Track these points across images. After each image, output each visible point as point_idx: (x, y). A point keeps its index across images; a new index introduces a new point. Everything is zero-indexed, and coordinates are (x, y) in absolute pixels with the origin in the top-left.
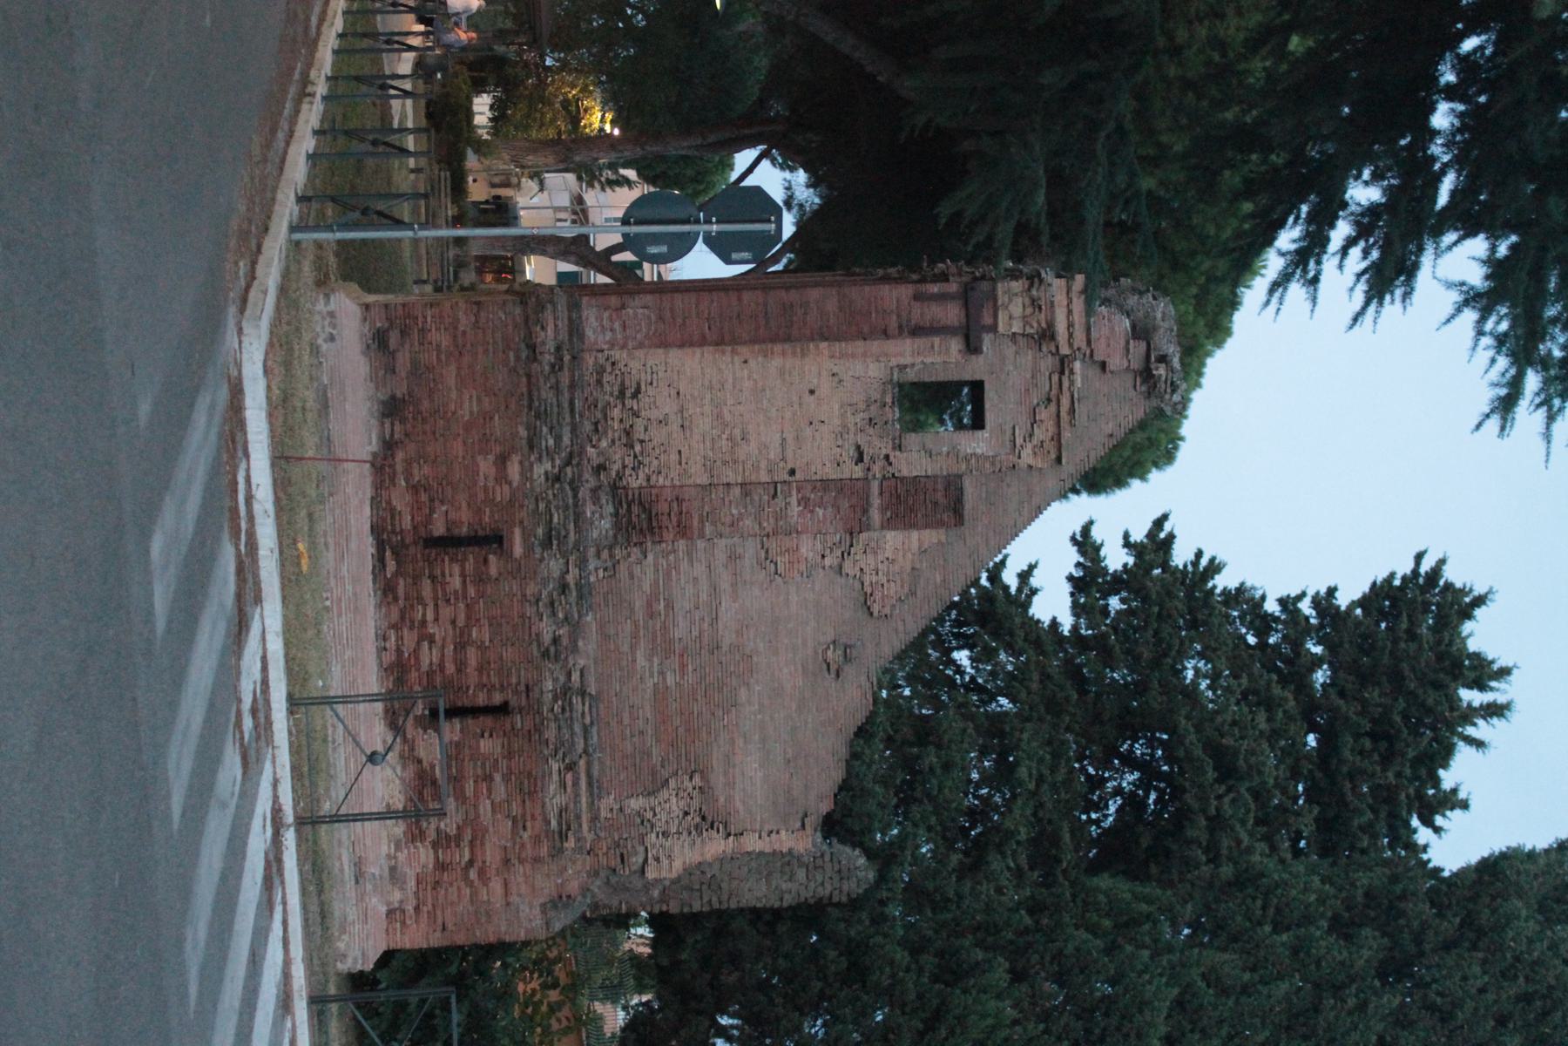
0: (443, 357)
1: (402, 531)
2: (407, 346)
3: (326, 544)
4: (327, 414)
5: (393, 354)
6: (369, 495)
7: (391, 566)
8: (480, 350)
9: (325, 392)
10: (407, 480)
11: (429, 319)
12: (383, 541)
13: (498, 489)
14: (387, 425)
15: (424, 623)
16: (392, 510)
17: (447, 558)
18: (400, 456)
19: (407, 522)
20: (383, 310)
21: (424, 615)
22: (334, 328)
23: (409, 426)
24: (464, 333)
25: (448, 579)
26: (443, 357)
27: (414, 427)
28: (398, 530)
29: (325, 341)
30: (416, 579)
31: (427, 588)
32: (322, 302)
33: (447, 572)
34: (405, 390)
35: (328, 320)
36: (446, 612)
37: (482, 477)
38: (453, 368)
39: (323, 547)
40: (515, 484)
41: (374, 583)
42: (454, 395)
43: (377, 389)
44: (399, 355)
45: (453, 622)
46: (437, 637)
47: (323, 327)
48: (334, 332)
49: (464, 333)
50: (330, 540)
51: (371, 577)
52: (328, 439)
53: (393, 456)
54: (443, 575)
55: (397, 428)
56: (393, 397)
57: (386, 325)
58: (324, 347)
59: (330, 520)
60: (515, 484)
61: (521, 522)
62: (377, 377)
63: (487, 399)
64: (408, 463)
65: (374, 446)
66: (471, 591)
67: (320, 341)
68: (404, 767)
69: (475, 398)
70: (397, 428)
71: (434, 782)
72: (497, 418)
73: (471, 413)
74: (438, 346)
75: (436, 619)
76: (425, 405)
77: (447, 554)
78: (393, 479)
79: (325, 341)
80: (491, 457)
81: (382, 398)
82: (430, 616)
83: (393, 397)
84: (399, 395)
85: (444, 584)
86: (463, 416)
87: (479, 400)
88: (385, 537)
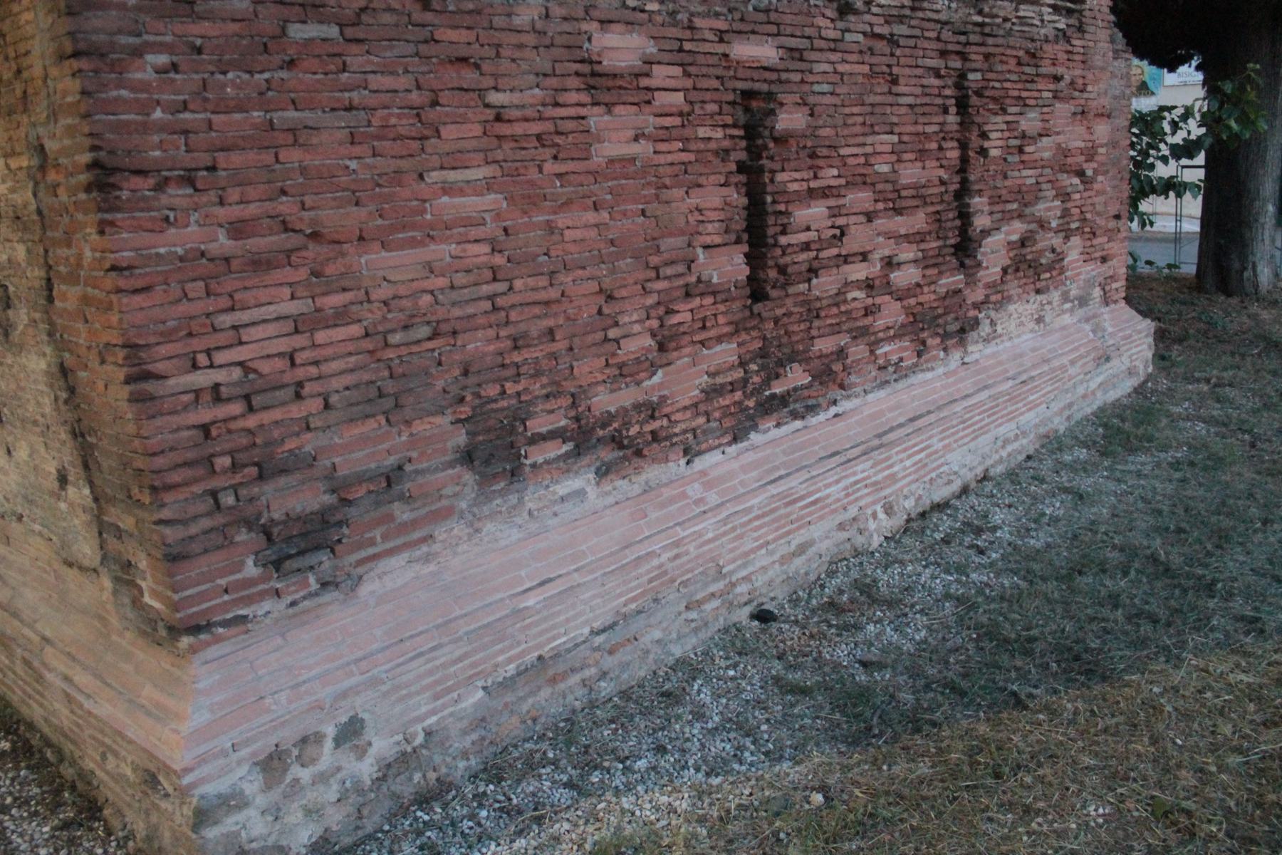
1: (742, 364)
2: (309, 443)
3: (802, 549)
4: (556, 656)
5: (340, 488)
6: (677, 466)
7: (796, 376)
8: (293, 156)
9: (507, 684)
10: (653, 368)
11: (202, 379)
12: (759, 404)
13: (662, 99)
14: (537, 455)
15: (869, 285)
16: (711, 393)
17: (783, 240)
18: (605, 401)
19: (726, 353)
20: (202, 565)
21: (857, 285)
22: (338, 742)
23: (537, 388)
24: (238, 229)
25: (812, 235)
27: (537, 374)
28: (739, 374)
30: (812, 312)
31: (825, 284)
32: (230, 823)
33: (803, 237)
34: (444, 421)
35: (296, 771)
36: (859, 237)
38: (372, 261)
39: (811, 552)
40: (651, 49)
41: (812, 409)
42: (443, 251)
43: (447, 513)
44: (347, 465)
45: (870, 217)
46: (887, 252)
47: (322, 778)
48: (330, 731)
49: (238, 229)
50: (797, 540)
51: (813, 420)
52: (612, 627)
53: (606, 420)
54: (806, 247)
55: (539, 424)
56: (468, 457)
57: (242, 536)
58: (382, 745)
59: (762, 559)
60: (651, 49)
61: (721, 37)
62: (414, 524)
63: (448, 132)
64: (624, 373)
65: (581, 480)
66: (830, 175)
67: (366, 769)
68: (1009, 299)
69: (452, 176)
70: (539, 424)
71: (1023, 243)
72: (495, 98)
73: (489, 186)
74: (299, 325)
75: (864, 256)
76: (478, 344)
77: (774, 236)
78: (651, 410)
79: (361, 752)
80: (597, 119)
81: (470, 492)
82: (858, 272)
83: (468, 457)
85: (822, 244)
86: (498, 216)
87: (453, 162)
88: (751, 403)
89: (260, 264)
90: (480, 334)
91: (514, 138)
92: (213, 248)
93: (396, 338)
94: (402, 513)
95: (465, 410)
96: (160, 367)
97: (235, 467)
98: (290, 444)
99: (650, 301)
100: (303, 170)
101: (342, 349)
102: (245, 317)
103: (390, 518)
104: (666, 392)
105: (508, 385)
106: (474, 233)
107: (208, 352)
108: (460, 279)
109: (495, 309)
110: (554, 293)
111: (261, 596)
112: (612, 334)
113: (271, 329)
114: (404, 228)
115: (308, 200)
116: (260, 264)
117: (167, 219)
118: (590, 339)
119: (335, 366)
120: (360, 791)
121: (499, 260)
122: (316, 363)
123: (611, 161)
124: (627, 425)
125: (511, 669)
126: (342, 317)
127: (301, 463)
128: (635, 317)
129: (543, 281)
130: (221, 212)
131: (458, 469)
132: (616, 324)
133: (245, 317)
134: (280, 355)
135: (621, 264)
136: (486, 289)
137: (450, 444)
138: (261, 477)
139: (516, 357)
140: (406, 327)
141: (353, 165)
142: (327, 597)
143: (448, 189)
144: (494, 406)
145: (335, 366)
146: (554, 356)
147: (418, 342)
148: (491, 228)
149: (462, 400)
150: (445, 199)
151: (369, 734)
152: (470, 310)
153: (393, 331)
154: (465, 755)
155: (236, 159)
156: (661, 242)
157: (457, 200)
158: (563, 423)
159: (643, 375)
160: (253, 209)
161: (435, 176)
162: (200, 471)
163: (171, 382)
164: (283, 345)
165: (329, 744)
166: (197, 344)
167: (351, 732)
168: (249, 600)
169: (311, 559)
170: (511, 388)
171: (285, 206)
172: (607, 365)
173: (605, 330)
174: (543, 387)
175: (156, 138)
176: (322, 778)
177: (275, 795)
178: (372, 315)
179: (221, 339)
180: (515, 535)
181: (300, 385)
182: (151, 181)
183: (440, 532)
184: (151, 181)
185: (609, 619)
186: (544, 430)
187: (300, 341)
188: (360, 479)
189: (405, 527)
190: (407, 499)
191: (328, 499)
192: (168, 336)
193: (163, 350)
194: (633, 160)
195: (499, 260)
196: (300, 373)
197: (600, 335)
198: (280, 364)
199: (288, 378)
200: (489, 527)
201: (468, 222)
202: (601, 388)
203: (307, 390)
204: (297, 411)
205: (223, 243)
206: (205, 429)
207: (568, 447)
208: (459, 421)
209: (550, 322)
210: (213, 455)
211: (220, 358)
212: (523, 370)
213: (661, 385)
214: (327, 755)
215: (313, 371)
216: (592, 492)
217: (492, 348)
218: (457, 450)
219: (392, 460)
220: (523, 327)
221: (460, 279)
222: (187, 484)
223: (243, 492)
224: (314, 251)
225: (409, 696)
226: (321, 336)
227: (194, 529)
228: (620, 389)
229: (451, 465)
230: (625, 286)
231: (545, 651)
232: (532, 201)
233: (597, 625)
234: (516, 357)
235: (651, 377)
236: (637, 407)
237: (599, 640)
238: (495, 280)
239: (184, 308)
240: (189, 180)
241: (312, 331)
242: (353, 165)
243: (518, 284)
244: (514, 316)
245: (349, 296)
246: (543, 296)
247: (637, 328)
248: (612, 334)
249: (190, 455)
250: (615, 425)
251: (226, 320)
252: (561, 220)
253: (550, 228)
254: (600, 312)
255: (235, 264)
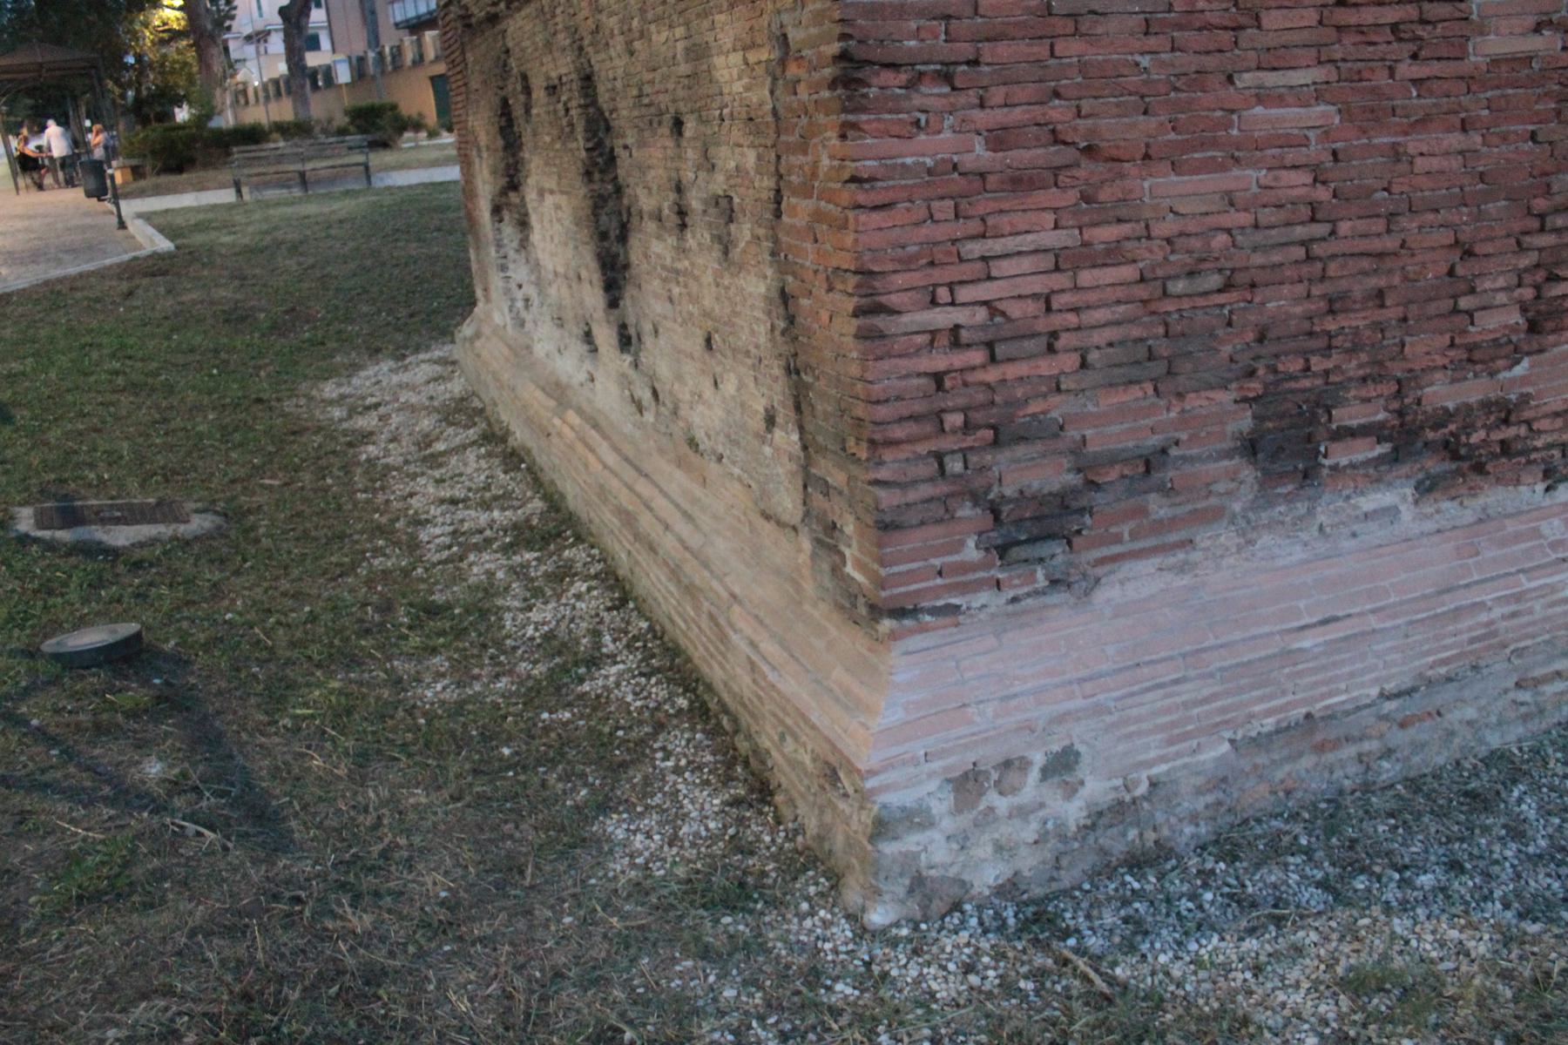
0: (1105, 234)
2: (1058, 408)
4: (1330, 716)
5: (1088, 468)
6: (1531, 492)
8: (1071, 49)
9: (1260, 742)
11: (942, 318)
14: (1342, 455)
18: (1441, 393)
20: (912, 541)
22: (1046, 773)
23: (1352, 367)
26: (1105, 234)
27: (1352, 351)
29: (1071, 790)
32: (911, 842)
34: (1226, 397)
35: (993, 798)
37: (1536, 43)
42: (1249, 178)
43: (1212, 516)
47: (1021, 813)
48: (1039, 759)
49: (998, 139)
52: (1409, 692)
55: (1350, 415)
56: (1251, 447)
57: (966, 511)
58: (1096, 788)
62: (1172, 523)
65: (1395, 495)
67: (1073, 812)
69: (1271, 79)
70: (1350, 415)
73: (1319, 93)
74: (1060, 261)
76: (1282, 303)
78: (1505, 412)
79: (1071, 790)
81: (1247, 493)
83: (1251, 447)
84: (1244, 422)
86: (1327, 134)
89: (1020, 182)
90: (1286, 289)
91: (1359, 29)
92: (968, 161)
93: (1179, 286)
94: (1159, 508)
95: (1255, 387)
96: (894, 300)
97: (968, 427)
98: (1034, 408)
99: (1525, 261)
100: (1083, 67)
101: (1110, 294)
102: (997, 246)
103: (1142, 511)
104: (1530, 390)
105: (1314, 360)
106: (1291, 156)
107: (951, 287)
108: (1267, 216)
109: (1309, 258)
110: (1390, 243)
111: (977, 586)
112: (1464, 303)
113: (1026, 264)
114: (1202, 146)
115: (1086, 106)
116: (1020, 182)
117: (917, 123)
118: (1432, 308)
119: (1100, 315)
120: (1063, 838)
121: (1322, 194)
122: (1075, 310)
123: (1495, 62)
124: (1468, 428)
125: (1269, 723)
126: (1113, 255)
127: (1049, 432)
128: (1501, 282)
129: (1379, 225)
130: (978, 114)
131: (1237, 460)
132: (1472, 291)
133: (997, 246)
134: (1035, 296)
135: (1490, 207)
136: (1300, 232)
137: (1231, 428)
138: (996, 443)
139: (1331, 325)
140: (1191, 274)
141: (1145, 61)
142: (1055, 598)
143: (1263, 97)
144: (1293, 385)
145: (1100, 315)
146: (1380, 327)
147: (1205, 294)
148: (1315, 151)
149: (1251, 373)
150: (1259, 110)
151: (1083, 771)
152: (1276, 258)
153: (1177, 277)
154: (1194, 818)
155: (1004, 50)
156: (1553, 178)
157: (1274, 111)
158: (1381, 416)
159: (1500, 363)
160: (1018, 114)
161: (1247, 79)
162: (928, 428)
163: (905, 318)
164: (1038, 285)
165: (1034, 774)
166: (938, 275)
167: (1062, 765)
168: (964, 588)
169: (1044, 549)
170: (1318, 363)
171: (1058, 112)
172: (1452, 345)
173: (1455, 297)
174: (1360, 366)
175: (913, 25)
176: (1021, 813)
177: (965, 820)
178: (1150, 255)
179: (966, 271)
180: (1298, 554)
181: (1054, 335)
182: (903, 77)
183: (1203, 537)
184: (903, 77)
185: (1408, 683)
186: (1354, 423)
187: (1061, 280)
188: (1112, 459)
189: (1160, 526)
190: (1167, 491)
191: (1073, 479)
192: (907, 264)
193: (900, 280)
194: (1528, 59)
195: (1322, 194)
196: (1057, 321)
197: (1446, 304)
198: (1032, 307)
199: (1042, 325)
200: (1266, 539)
201: (1289, 142)
202: (1438, 375)
203: (1064, 340)
204: (1047, 367)
205: (979, 154)
206: (938, 378)
207: (1384, 449)
208: (1245, 400)
209: (1382, 283)
210: (943, 411)
211: (964, 294)
212: (1337, 342)
213: (1524, 380)
214: (1030, 787)
215: (1072, 319)
216: (1407, 512)
217: (1298, 310)
218: (1239, 436)
219: (1155, 441)
220: (1344, 284)
221: (1267, 216)
222: (910, 441)
223: (973, 459)
224: (1088, 170)
225: (1139, 734)
226: (1086, 277)
227: (912, 496)
228: (1466, 379)
229: (1228, 454)
230: (1492, 239)
231: (1317, 708)
232: (1373, 115)
233: (1390, 687)
234: (1331, 325)
235: (1510, 368)
236: (1486, 405)
237: (1390, 706)
238: (1313, 220)
239: (927, 231)
240: (947, 78)
241: (1076, 269)
242: (1145, 61)
243: (1344, 227)
244: (1333, 269)
245: (1125, 229)
246: (1376, 245)
247: (1501, 298)
248: (1464, 303)
249: (919, 407)
250: (1452, 427)
251: (975, 249)
252: (1413, 144)
253: (1396, 153)
254: (1451, 272)
255: (992, 180)
